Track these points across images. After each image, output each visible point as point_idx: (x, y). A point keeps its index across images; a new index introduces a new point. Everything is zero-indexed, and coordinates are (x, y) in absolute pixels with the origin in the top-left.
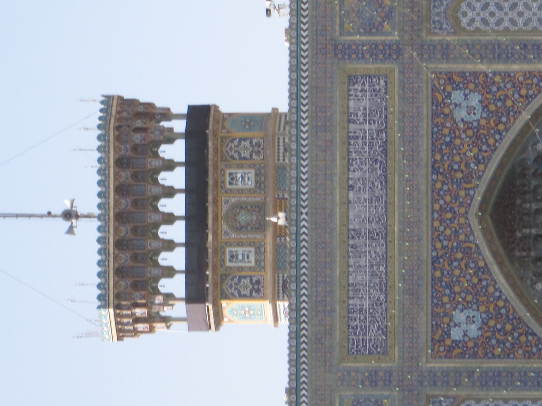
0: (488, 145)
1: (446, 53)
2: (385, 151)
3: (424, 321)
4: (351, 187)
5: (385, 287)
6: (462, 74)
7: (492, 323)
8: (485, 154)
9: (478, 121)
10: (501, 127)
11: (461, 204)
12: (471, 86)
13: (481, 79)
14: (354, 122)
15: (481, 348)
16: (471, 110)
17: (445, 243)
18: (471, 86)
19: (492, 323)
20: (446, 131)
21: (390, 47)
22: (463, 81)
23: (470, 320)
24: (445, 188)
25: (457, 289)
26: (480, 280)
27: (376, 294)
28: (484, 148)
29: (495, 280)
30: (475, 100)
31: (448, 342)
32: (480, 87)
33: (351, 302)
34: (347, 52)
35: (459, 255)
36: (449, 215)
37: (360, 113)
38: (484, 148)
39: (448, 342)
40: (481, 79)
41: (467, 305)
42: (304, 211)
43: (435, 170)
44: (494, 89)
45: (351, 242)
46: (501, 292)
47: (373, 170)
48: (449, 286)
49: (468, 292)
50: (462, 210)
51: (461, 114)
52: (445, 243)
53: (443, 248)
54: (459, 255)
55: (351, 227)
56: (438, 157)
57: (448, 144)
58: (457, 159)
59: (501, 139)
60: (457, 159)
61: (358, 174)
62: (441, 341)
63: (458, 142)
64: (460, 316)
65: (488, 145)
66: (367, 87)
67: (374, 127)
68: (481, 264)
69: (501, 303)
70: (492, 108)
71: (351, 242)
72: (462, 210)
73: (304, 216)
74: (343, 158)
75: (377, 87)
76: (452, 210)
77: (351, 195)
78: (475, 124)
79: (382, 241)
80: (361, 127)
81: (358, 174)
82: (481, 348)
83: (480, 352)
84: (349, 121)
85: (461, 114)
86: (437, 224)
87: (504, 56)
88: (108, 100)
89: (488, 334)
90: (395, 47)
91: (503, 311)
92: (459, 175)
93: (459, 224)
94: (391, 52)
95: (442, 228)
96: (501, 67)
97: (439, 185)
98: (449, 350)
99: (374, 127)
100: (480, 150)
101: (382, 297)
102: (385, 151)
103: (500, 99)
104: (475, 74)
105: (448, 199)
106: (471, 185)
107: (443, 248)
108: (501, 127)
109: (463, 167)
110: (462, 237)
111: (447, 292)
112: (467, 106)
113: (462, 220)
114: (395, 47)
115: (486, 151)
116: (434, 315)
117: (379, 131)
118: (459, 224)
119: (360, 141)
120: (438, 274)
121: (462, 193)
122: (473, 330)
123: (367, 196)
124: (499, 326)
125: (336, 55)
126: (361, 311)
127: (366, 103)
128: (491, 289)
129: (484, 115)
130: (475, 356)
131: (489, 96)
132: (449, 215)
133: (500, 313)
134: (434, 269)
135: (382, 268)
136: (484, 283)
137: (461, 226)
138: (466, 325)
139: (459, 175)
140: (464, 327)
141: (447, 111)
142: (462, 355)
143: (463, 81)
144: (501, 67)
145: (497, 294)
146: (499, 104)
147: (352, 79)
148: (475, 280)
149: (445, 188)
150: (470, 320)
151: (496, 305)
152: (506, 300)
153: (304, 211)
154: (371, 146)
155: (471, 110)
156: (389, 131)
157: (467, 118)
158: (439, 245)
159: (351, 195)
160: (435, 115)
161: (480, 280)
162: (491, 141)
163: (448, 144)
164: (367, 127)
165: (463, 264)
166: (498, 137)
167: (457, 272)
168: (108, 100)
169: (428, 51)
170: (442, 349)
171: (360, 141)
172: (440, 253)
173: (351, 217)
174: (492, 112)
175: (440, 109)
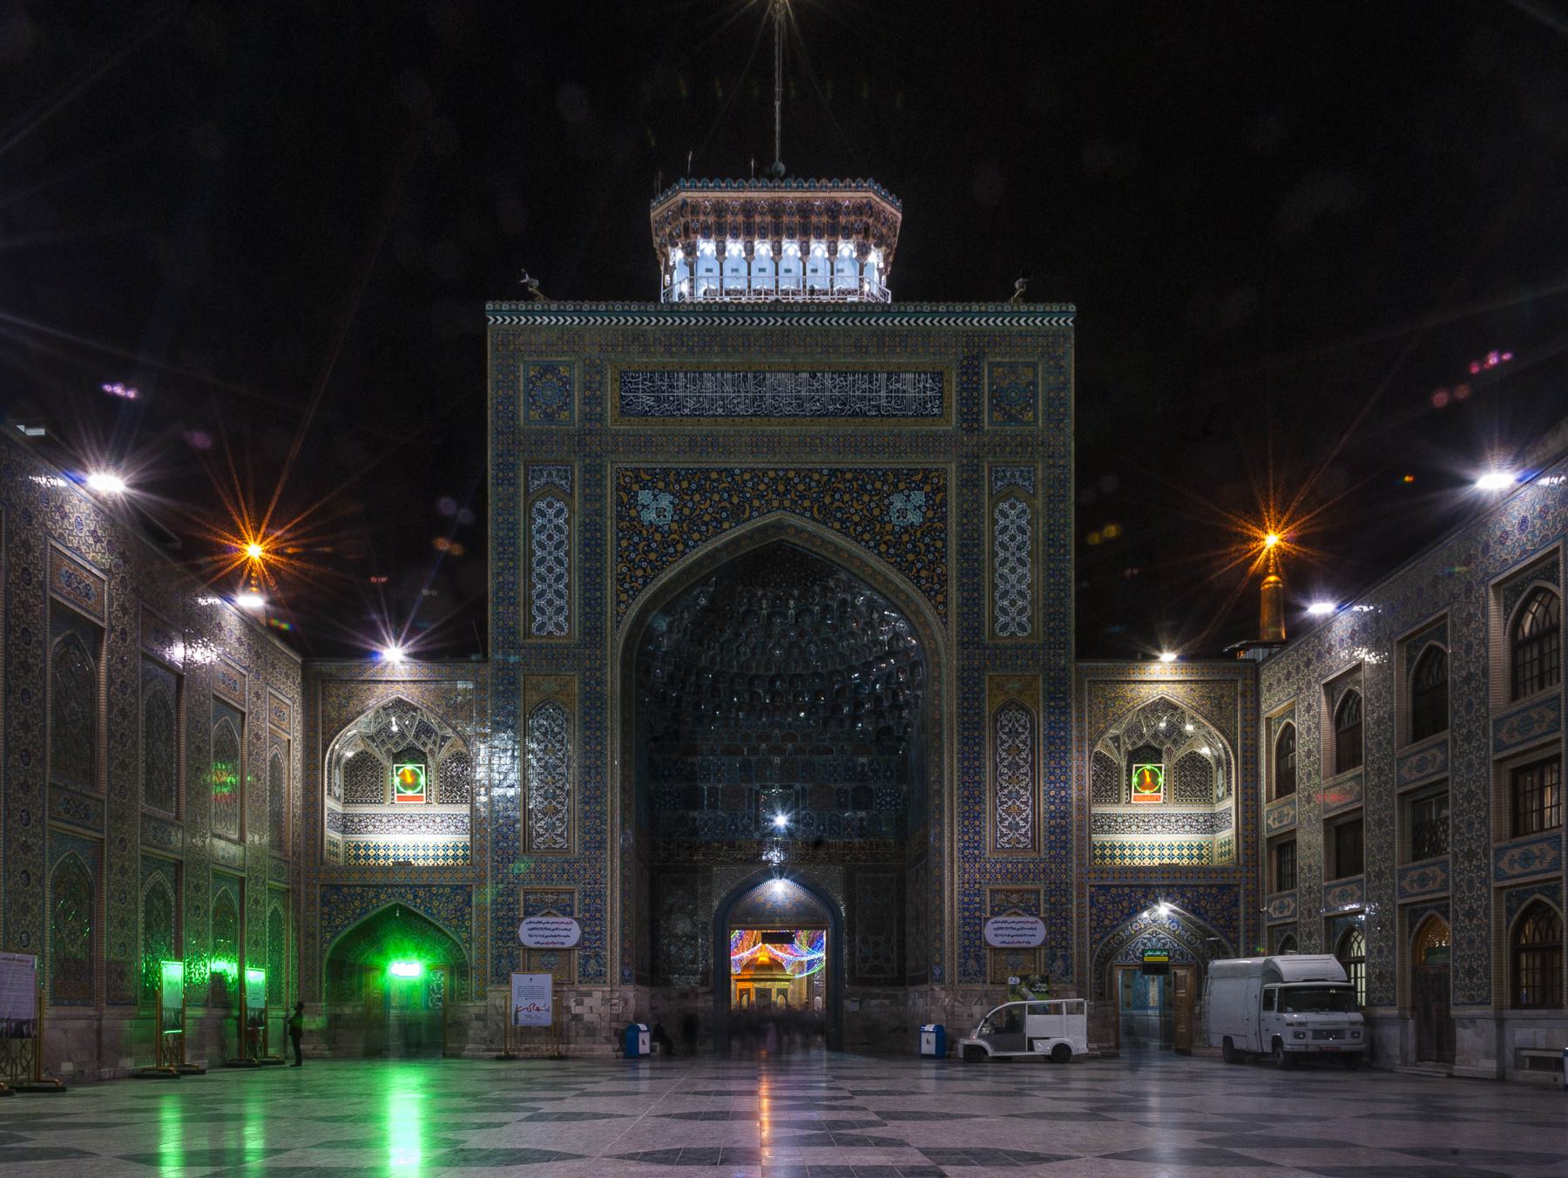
0: (862, 533)
1: (970, 483)
2: (855, 414)
3: (660, 461)
4: (813, 376)
6: (944, 503)
10: (883, 548)
11: (794, 502)
12: (930, 514)
13: (938, 525)
14: (889, 379)
17: (750, 484)
18: (930, 514)
19: (658, 537)
20: (878, 485)
21: (977, 420)
23: (660, 512)
24: (813, 484)
26: (706, 524)
27: (691, 404)
28: (859, 529)
30: (914, 518)
31: (635, 487)
34: (970, 370)
35: (735, 500)
36: (781, 488)
38: (859, 529)
39: (635, 487)
40: (938, 525)
41: (677, 510)
43: (833, 473)
44: (927, 540)
47: (833, 401)
48: (700, 488)
49: (692, 510)
51: (898, 502)
52: (750, 484)
53: (744, 482)
56: (849, 476)
57: (863, 487)
58: (847, 497)
60: (847, 497)
61: (828, 383)
62: (637, 479)
63: (866, 498)
64: (665, 501)
65: (862, 533)
67: (883, 402)
68: (726, 525)
69: (680, 547)
70: (905, 538)
72: (787, 504)
76: (787, 491)
77: (805, 375)
81: (828, 383)
83: (624, 524)
84: (890, 373)
85: (898, 502)
86: (772, 474)
91: (671, 550)
92: (828, 500)
95: (766, 480)
96: (953, 545)
97: (816, 476)
98: (626, 489)
99: (883, 402)
101: (687, 411)
102: (855, 414)
104: (943, 518)
107: (744, 482)
108: (883, 548)
109: (837, 504)
110: (756, 503)
113: (776, 503)
116: (666, 471)
117: (878, 408)
119: (866, 386)
120: (714, 476)
121: (807, 503)
122: (649, 516)
124: (654, 545)
125: (966, 358)
126: (671, 386)
130: (620, 518)
132: (781, 488)
134: (720, 472)
135: (720, 411)
136: (703, 528)
137: (769, 502)
138: (656, 508)
139: (828, 500)
140: (654, 505)
141: (902, 486)
142: (620, 503)
144: (953, 545)
145: (691, 543)
146: (909, 546)
147: (938, 376)
148: (707, 518)
149: (813, 484)
152: (683, 553)
154: (862, 399)
155: (902, 513)
157: (893, 509)
158: (747, 476)
159: (805, 375)
160: (896, 472)
161: (706, 524)
162: (867, 536)
163: (863, 487)
164: (883, 393)
165: (726, 504)
166: (872, 544)
167: (716, 497)
171: (866, 386)
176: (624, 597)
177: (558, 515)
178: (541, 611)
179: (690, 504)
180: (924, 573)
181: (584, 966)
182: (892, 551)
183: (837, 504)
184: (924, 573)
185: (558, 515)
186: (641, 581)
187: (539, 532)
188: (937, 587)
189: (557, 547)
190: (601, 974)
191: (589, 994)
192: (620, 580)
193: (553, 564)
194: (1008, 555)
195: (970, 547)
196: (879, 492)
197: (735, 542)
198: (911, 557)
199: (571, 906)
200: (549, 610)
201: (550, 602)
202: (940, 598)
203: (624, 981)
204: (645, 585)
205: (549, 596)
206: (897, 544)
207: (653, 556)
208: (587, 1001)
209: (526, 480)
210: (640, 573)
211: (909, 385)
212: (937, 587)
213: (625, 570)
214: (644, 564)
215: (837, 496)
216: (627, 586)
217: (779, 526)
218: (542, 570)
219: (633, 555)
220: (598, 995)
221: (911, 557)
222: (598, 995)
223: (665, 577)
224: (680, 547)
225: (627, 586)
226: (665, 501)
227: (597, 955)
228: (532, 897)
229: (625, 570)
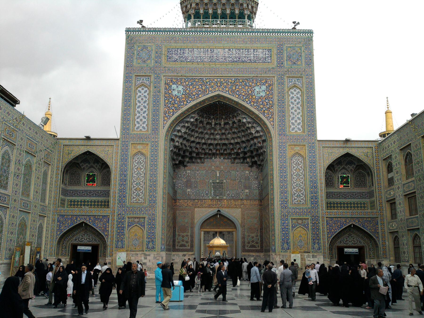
2: (243, 62)
5: (192, 62)
6: (272, 90)
7: (178, 99)
8: (242, 98)
9: (255, 95)
10: (252, 103)
11: (223, 89)
12: (268, 93)
15: (168, 96)
16: (259, 93)
18: (268, 93)
19: (178, 99)
20: (251, 84)
22: (270, 87)
23: (179, 92)
24: (229, 83)
25: (191, 87)
27: (190, 58)
28: (244, 97)
30: (263, 94)
33: (187, 49)
35: (204, 88)
36: (219, 85)
37: (257, 53)
38: (244, 97)
42: (221, 34)
44: (267, 101)
45: (209, 50)
49: (189, 91)
50: (221, 89)
51: (257, 89)
53: (207, 82)
54: (204, 88)
55: (215, 50)
57: (246, 84)
58: (240, 87)
60: (240, 87)
61: (234, 52)
63: (247, 88)
64: (181, 88)
66: (267, 56)
67: (252, 58)
68: (200, 96)
69: (185, 103)
70: (260, 100)
71: (209, 50)
72: (221, 89)
73: (219, 34)
74: (240, 47)
75: (267, 59)
77: (227, 50)
78: (253, 94)
79: (209, 61)
80: (252, 53)
81: (234, 52)
82: (168, 96)
84: (254, 49)
85: (257, 89)
87: (280, 104)
88: (311, 32)
89: (174, 98)
90: (282, 65)
91: (182, 104)
92: (234, 88)
93: (215, 88)
94: (280, 64)
95: (214, 82)
100: (243, 96)
101: (188, 60)
102: (243, 62)
103: (263, 103)
104: (272, 94)
105: (225, 84)
106: (230, 93)
107: (207, 82)
108: (252, 103)
109: (237, 89)
110: (210, 89)
111: (190, 84)
112: (260, 91)
113: (217, 89)
114: (282, 65)
117: (250, 60)
118: (215, 88)
121: (227, 89)
122: (175, 93)
123: (226, 55)
124: (176, 102)
126: (184, 53)
127: (261, 55)
128: (190, 99)
129: (257, 97)
131: (264, 99)
136: (193, 97)
137: (215, 89)
138: (178, 90)
139: (234, 88)
140: (177, 89)
141: (258, 84)
142: (166, 89)
143: (270, 87)
145: (189, 101)
146: (261, 103)
147: (270, 50)
148: (194, 94)
149: (229, 83)
150: (179, 92)
152: (186, 105)
153: (221, 34)
156: (251, 63)
157: (255, 91)
161: (194, 95)
162: (247, 100)
164: (252, 56)
165: (200, 89)
167: (197, 87)
168: (311, 32)
169: (281, 77)
170: (168, 81)
172: (204, 81)
173: (218, 50)
175: (260, 81)
176: (166, 118)
177: (145, 92)
178: (138, 123)
179: (189, 89)
180: (266, 112)
181: (147, 245)
182: (255, 104)
183: (237, 89)
185: (145, 92)
187: (145, 111)
188: (270, 116)
189: (144, 102)
190: (153, 248)
191: (149, 255)
192: (165, 114)
193: (143, 108)
194: (294, 106)
195: (282, 102)
196: (251, 86)
197: (204, 101)
198: (261, 106)
199: (144, 223)
200: (141, 123)
201: (141, 120)
202: (271, 119)
203: (162, 251)
204: (173, 114)
205: (141, 118)
206: (258, 102)
207: (176, 105)
208: (148, 257)
209: (135, 81)
210: (171, 111)
211: (260, 54)
212: (270, 116)
213: (166, 110)
214: (173, 108)
215: (237, 87)
216: (167, 115)
217: (219, 96)
218: (139, 110)
219: (169, 105)
220: (152, 256)
221: (261, 106)
222: (152, 256)
223: (180, 112)
224: (185, 103)
225: (167, 115)
226: (181, 88)
227: (152, 241)
228: (130, 220)
229: (166, 110)
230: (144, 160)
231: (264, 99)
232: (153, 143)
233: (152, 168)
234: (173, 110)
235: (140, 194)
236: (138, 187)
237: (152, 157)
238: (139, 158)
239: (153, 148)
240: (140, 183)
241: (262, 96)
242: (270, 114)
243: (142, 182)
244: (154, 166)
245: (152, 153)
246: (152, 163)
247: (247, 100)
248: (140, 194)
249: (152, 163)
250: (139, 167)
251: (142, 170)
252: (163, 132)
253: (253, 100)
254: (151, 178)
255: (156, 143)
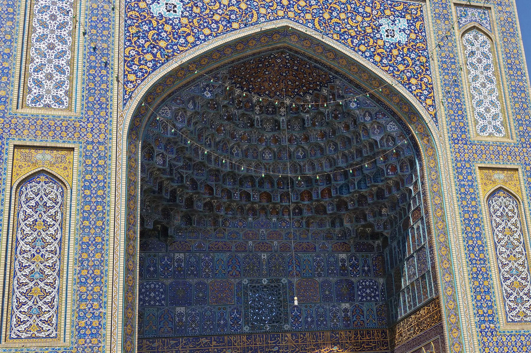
12: (413, 36)
18: (413, 36)
29: (217, 36)
32: (412, 43)
44: (413, 56)
46: (204, 40)
59: (366, 57)
69: (191, 39)
70: (395, 52)
78: (378, 36)
87: (445, 66)
91: (182, 41)
104: (424, 41)
108: (377, 58)
115: (352, 42)
129: (387, 45)
131: (405, 50)
133: (180, 37)
145: (202, 37)
151: (189, 34)
152: (194, 45)
166: (367, 54)
174: (391, 51)
176: (132, 77)
180: (413, 81)
182: (385, 61)
184: (413, 81)
186: (150, 65)
188: (426, 92)
192: (128, 62)
194: (478, 73)
197: (244, 41)
198: (401, 67)
202: (429, 102)
206: (389, 56)
212: (426, 92)
221: (401, 67)
224: (191, 39)
230: (59, 200)
231: (405, 50)
232: (89, 147)
233: (87, 223)
234: (155, 56)
235: (45, 308)
236: (36, 284)
237: (89, 188)
238: (42, 193)
239: (89, 162)
240: (42, 272)
241: (399, 42)
242: (424, 87)
243: (52, 267)
244: (93, 216)
245: (88, 177)
246: (87, 208)
247: (363, 48)
248: (45, 308)
249: (87, 208)
250: (40, 221)
251: (52, 231)
252: (122, 117)
253: (380, 51)
254: (85, 256)
255: (102, 148)
